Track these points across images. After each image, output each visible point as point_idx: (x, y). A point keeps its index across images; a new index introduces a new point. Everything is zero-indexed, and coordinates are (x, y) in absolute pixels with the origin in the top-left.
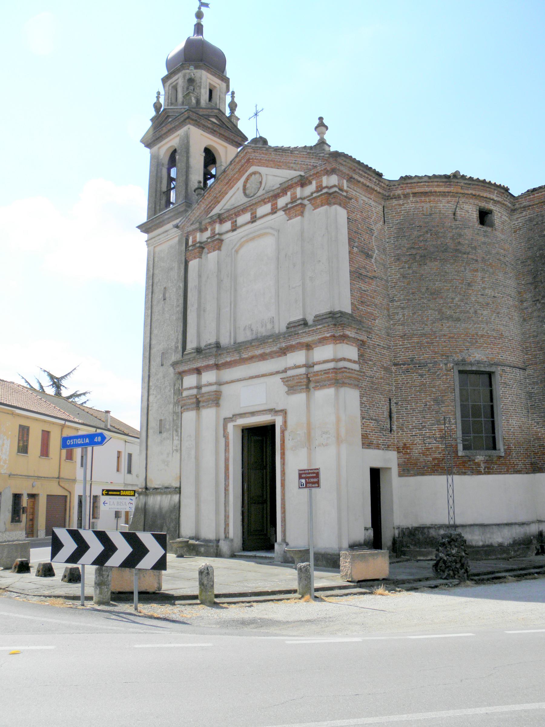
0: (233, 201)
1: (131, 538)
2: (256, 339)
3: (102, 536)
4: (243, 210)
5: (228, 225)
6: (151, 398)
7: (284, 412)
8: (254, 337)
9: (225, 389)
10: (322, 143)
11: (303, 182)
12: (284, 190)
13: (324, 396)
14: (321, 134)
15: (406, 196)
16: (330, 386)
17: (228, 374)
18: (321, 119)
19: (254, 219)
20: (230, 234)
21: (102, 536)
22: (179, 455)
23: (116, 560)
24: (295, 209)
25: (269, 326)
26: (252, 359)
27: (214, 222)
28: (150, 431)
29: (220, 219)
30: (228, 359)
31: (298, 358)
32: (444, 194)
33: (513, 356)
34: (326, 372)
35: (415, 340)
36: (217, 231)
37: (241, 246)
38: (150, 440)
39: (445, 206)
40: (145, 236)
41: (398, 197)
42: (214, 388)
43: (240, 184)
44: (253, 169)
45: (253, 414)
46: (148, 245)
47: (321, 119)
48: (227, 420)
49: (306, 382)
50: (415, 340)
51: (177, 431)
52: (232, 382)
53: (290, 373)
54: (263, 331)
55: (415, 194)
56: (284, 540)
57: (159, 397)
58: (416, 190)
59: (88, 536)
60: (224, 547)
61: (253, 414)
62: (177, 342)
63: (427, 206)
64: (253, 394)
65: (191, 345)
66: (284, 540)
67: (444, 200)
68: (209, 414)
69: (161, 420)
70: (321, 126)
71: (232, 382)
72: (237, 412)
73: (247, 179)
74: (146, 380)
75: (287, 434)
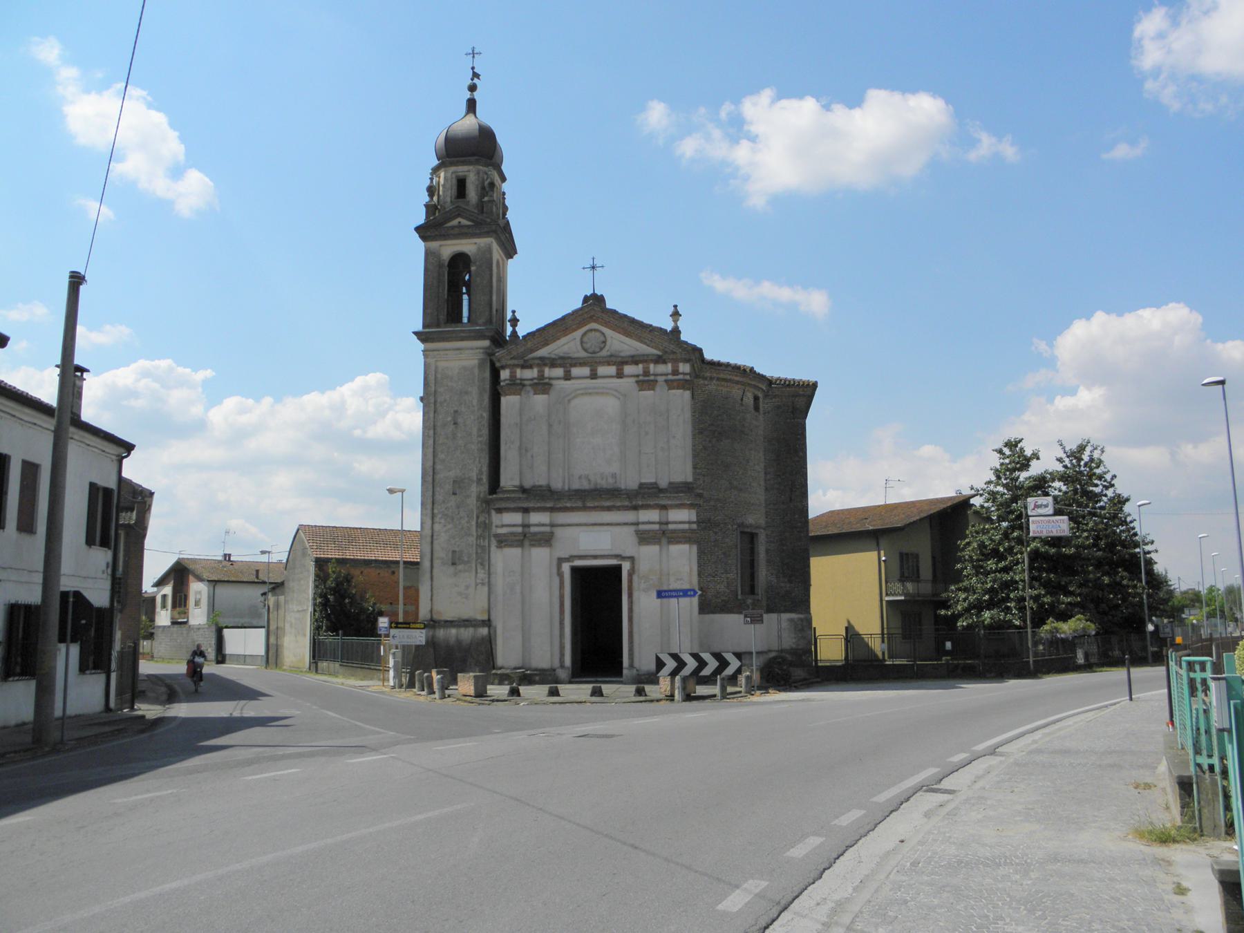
0: (565, 349)
1: (695, 656)
2: (596, 490)
3: (675, 657)
4: (581, 363)
5: (559, 372)
6: (437, 527)
7: (632, 559)
8: (592, 486)
9: (559, 532)
10: (676, 331)
11: (659, 360)
12: (634, 360)
13: (676, 549)
14: (675, 321)
15: (712, 379)
16: (685, 543)
17: (562, 518)
18: (675, 306)
19: (594, 376)
20: (562, 382)
21: (675, 657)
22: (486, 589)
23: (686, 671)
24: (646, 383)
25: (611, 480)
26: (594, 508)
27: (545, 365)
28: (437, 563)
29: (553, 363)
30: (568, 505)
31: (653, 515)
32: (737, 383)
33: (762, 522)
34: (683, 531)
35: (712, 503)
36: (546, 375)
37: (574, 397)
38: (435, 571)
39: (736, 391)
40: (421, 346)
41: (705, 378)
42: (547, 529)
43: (578, 334)
44: (594, 325)
45: (595, 557)
46: (425, 356)
47: (675, 306)
48: (561, 561)
49: (663, 536)
50: (712, 503)
51: (482, 564)
52: (569, 525)
53: (641, 527)
54: (604, 484)
55: (718, 379)
56: (631, 666)
57: (450, 526)
58: (722, 376)
59: (706, 656)
60: (563, 674)
61: (595, 557)
62: (481, 472)
63: (725, 390)
64: (595, 539)
65: (509, 478)
66: (631, 666)
67: (737, 387)
68: (540, 556)
69: (454, 552)
70: (676, 314)
71: (569, 525)
72: (575, 553)
73: (585, 334)
74: (429, 506)
75: (635, 578)
